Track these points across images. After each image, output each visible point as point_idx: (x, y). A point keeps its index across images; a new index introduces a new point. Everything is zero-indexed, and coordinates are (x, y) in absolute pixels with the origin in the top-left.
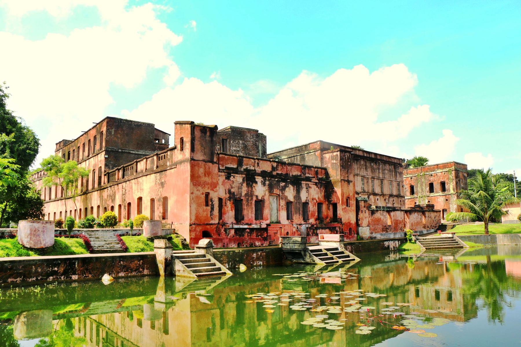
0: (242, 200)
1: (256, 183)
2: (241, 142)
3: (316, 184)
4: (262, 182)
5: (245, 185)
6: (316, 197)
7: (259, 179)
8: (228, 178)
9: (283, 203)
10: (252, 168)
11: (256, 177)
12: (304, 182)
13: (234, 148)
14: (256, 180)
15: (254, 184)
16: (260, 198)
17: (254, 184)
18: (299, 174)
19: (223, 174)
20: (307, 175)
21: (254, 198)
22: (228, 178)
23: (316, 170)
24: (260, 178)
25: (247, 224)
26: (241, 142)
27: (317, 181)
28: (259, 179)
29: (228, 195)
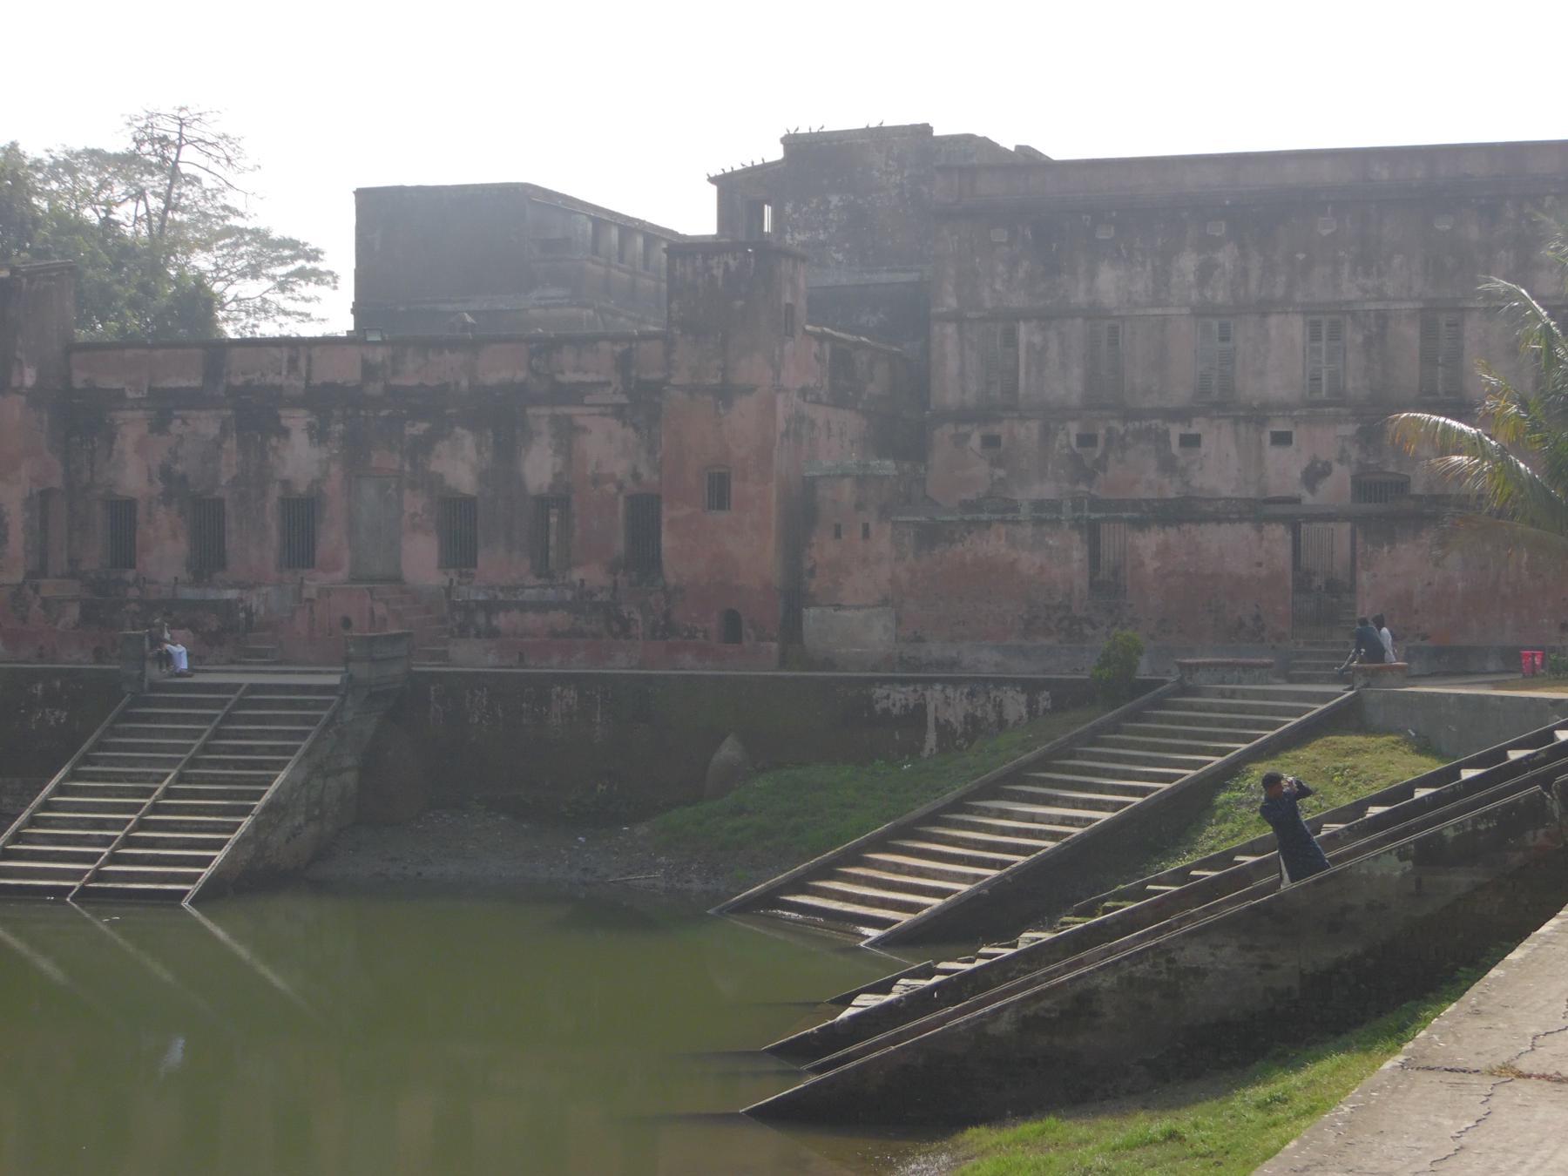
0: (221, 501)
1: (285, 433)
2: (835, 200)
3: (619, 412)
4: (311, 427)
5: (231, 444)
6: (620, 468)
7: (297, 421)
8: (160, 425)
9: (414, 503)
10: (271, 379)
11: (283, 413)
12: (545, 411)
13: (800, 237)
14: (283, 422)
15: (274, 441)
16: (302, 489)
17: (274, 441)
18: (521, 375)
19: (140, 414)
20: (570, 377)
21: (275, 492)
22: (160, 425)
23: (618, 349)
24: (302, 413)
25: (237, 585)
26: (835, 200)
27: (624, 400)
28: (297, 421)
29: (160, 486)
